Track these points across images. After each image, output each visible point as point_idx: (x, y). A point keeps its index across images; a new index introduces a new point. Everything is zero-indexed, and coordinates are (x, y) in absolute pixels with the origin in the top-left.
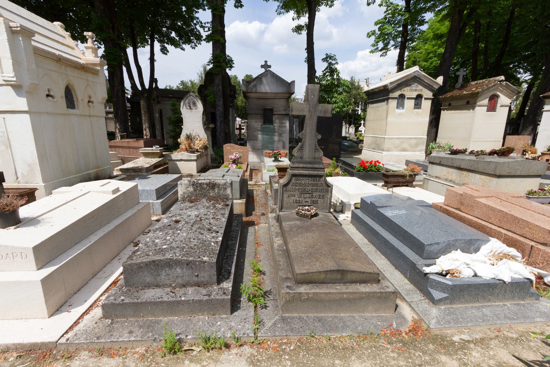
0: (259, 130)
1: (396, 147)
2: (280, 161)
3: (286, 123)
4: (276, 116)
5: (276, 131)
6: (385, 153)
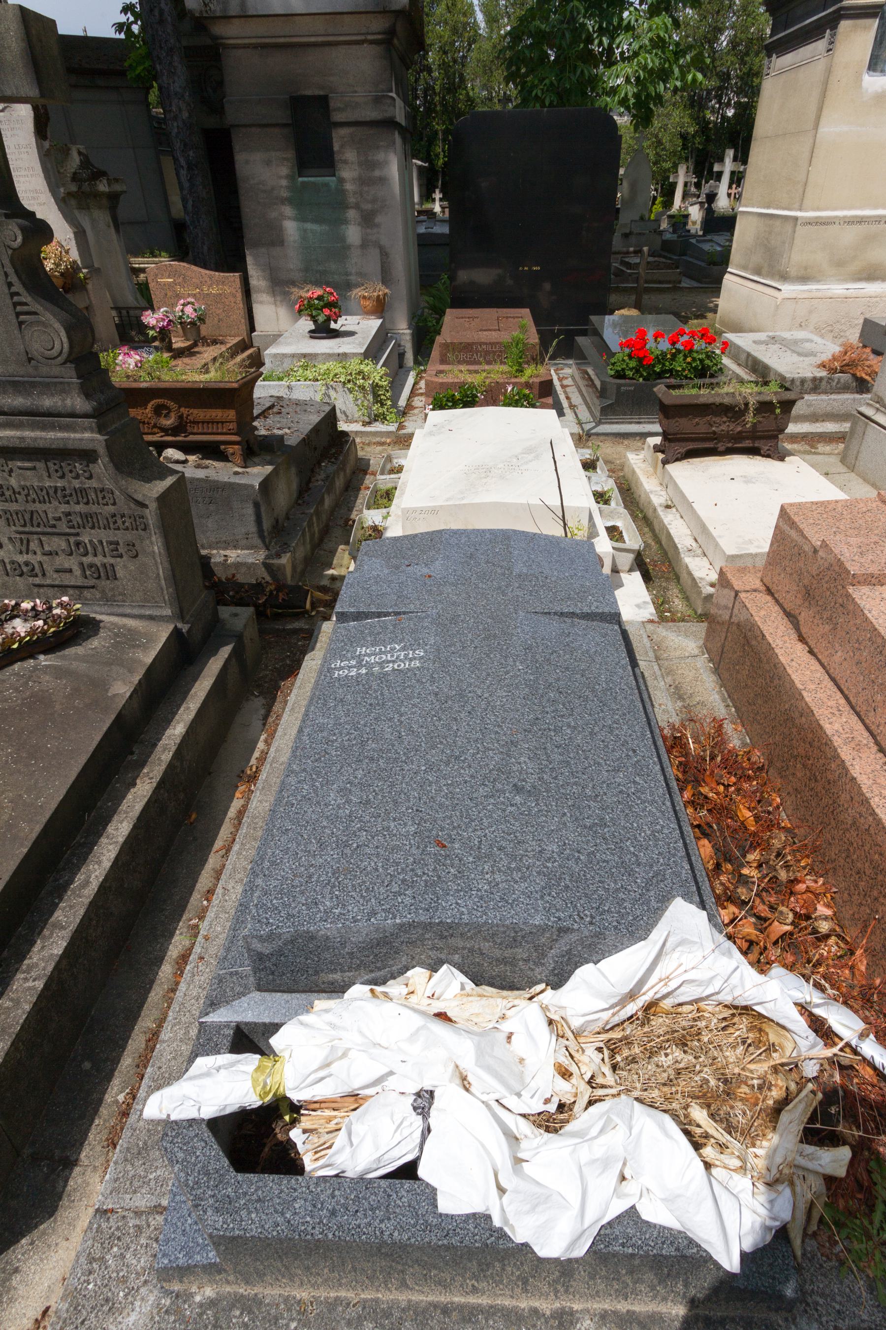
0: (283, 201)
1: (839, 264)
2: (335, 334)
3: (386, 163)
4: (344, 131)
5: (352, 200)
6: (789, 289)
